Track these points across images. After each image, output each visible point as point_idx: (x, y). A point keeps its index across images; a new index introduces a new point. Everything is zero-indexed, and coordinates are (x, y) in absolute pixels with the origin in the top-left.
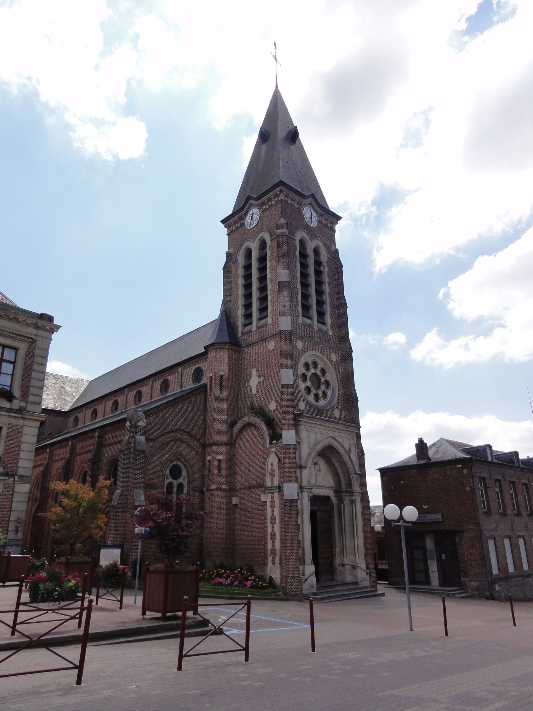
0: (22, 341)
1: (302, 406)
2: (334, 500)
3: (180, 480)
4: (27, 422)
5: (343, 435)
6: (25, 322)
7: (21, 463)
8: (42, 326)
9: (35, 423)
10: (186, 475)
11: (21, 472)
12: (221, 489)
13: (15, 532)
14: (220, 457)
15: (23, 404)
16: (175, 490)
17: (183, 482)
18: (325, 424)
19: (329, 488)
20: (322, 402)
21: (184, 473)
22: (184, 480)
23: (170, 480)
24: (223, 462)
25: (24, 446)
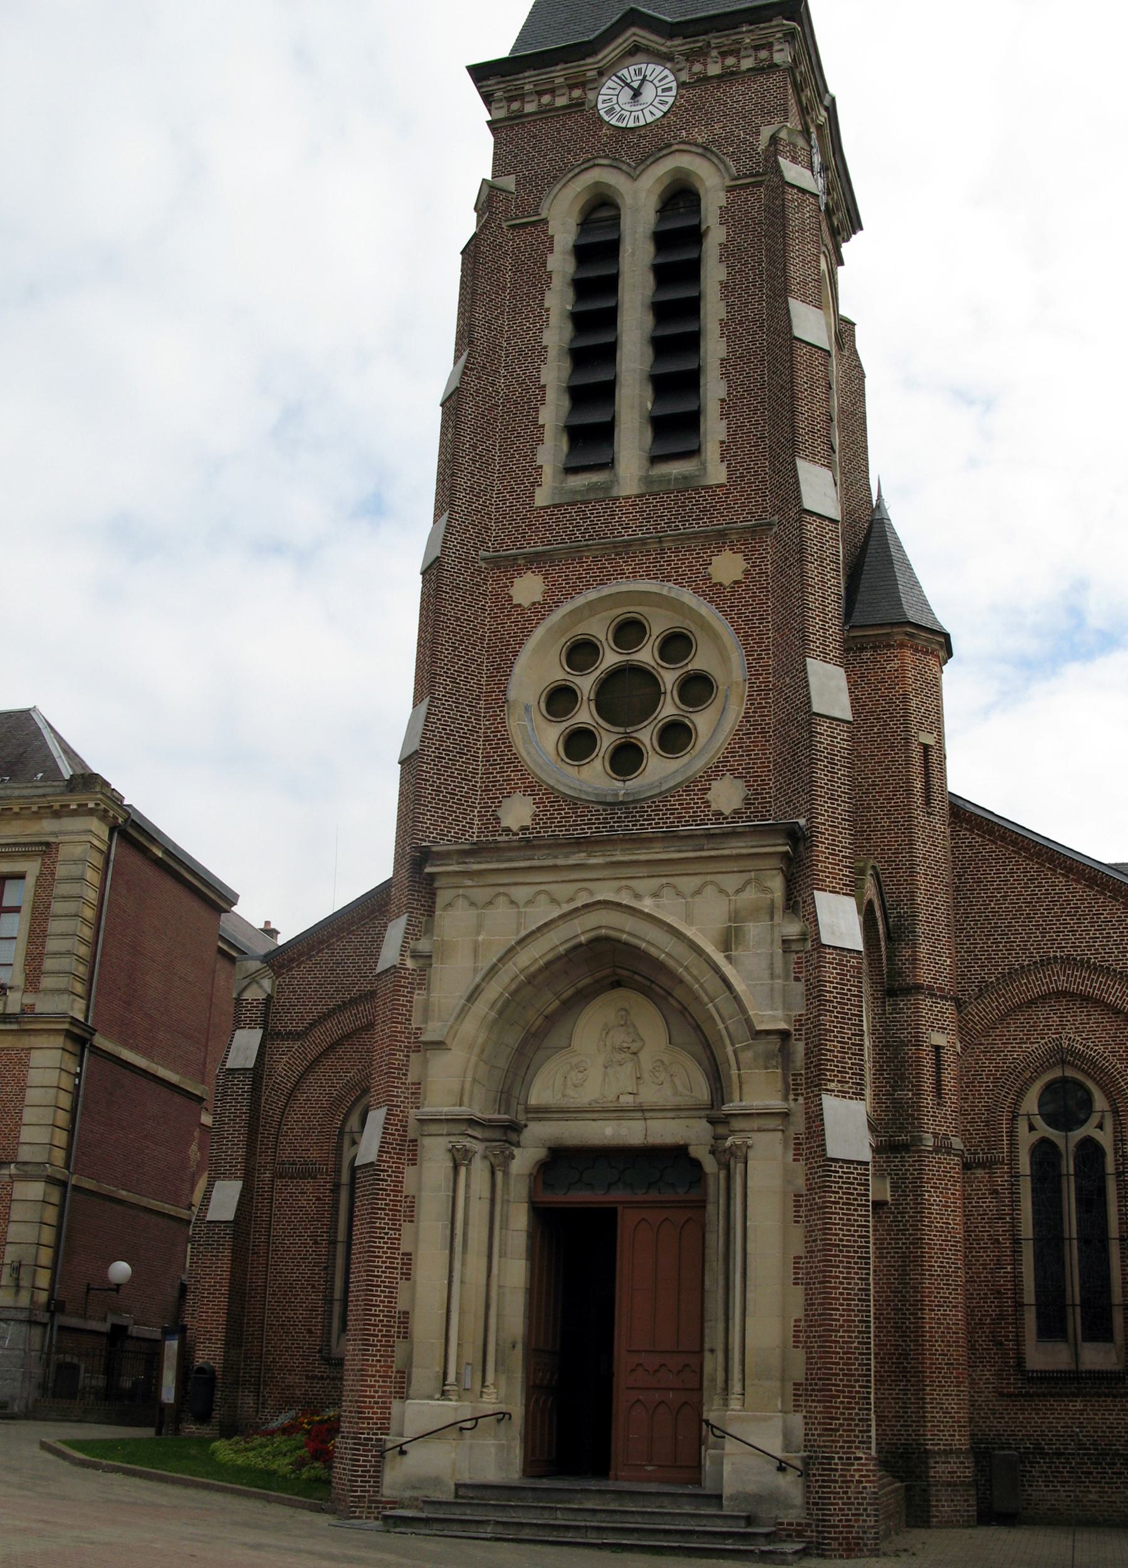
0: (25, 855)
1: (727, 795)
2: (710, 1165)
3: (1088, 1130)
4: (36, 1041)
5: (688, 884)
6: (48, 810)
7: (26, 1135)
8: (61, 806)
9: (52, 1038)
10: (1106, 1107)
11: (25, 1154)
12: (949, 1150)
13: (13, 1291)
14: (939, 1039)
15: (28, 999)
16: (1069, 1166)
17: (1098, 1135)
18: (560, 862)
19: (678, 1111)
20: (659, 770)
21: (1100, 1102)
22: (1100, 1126)
23: (1045, 1130)
24: (948, 1058)
25: (33, 1096)
